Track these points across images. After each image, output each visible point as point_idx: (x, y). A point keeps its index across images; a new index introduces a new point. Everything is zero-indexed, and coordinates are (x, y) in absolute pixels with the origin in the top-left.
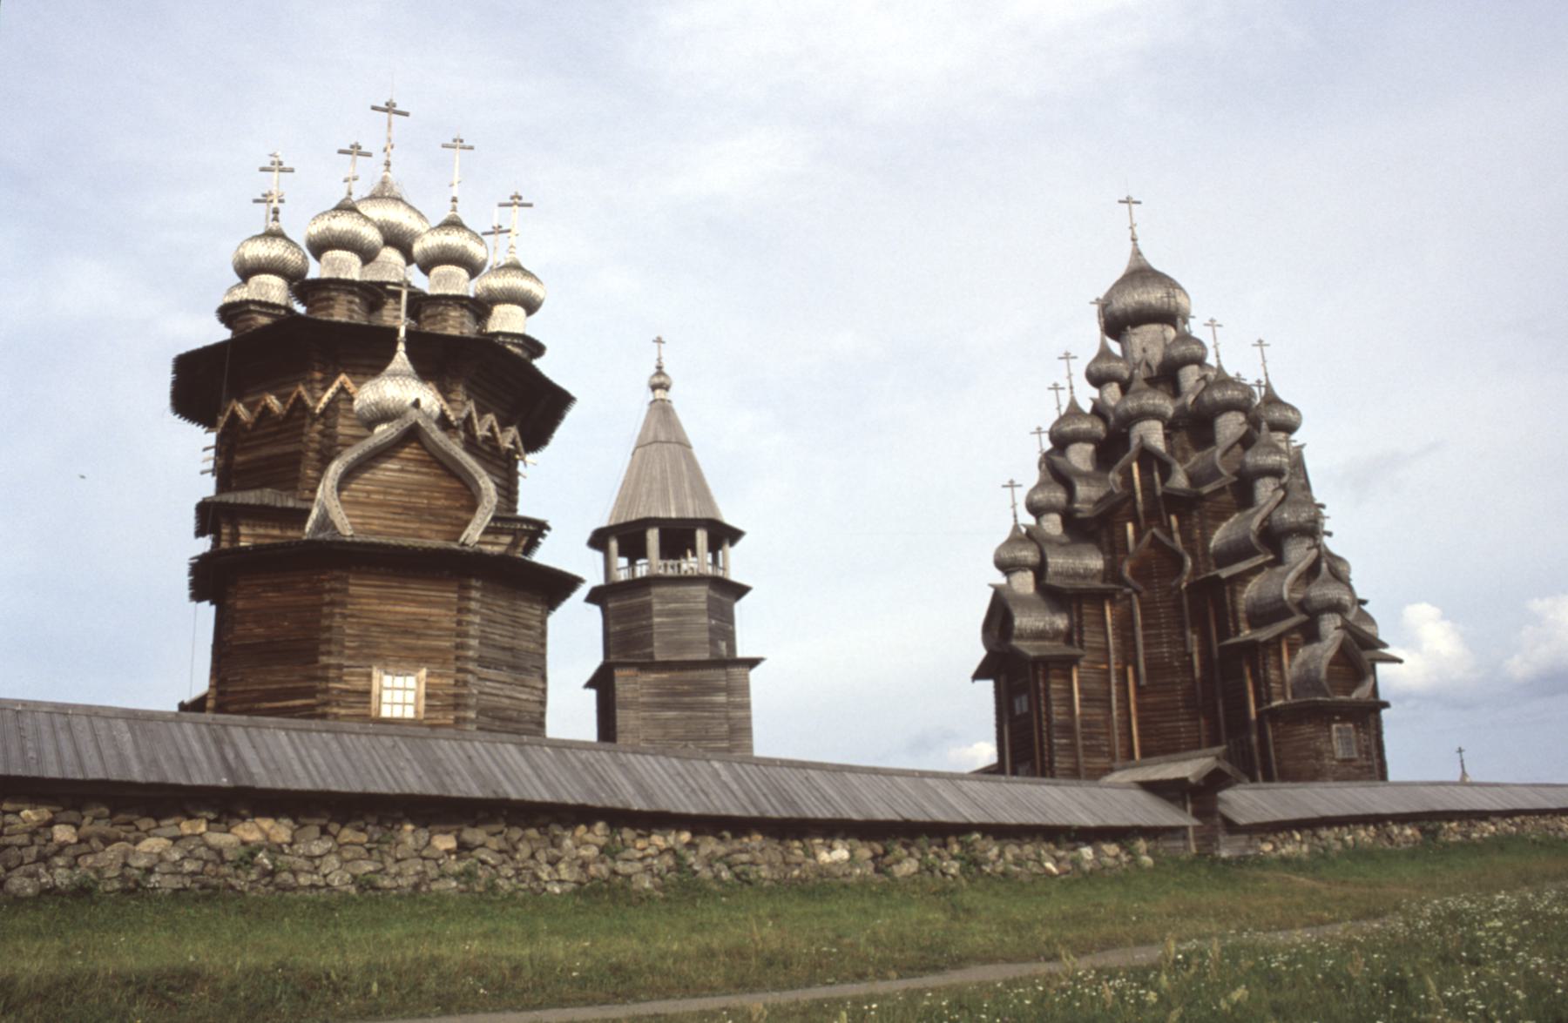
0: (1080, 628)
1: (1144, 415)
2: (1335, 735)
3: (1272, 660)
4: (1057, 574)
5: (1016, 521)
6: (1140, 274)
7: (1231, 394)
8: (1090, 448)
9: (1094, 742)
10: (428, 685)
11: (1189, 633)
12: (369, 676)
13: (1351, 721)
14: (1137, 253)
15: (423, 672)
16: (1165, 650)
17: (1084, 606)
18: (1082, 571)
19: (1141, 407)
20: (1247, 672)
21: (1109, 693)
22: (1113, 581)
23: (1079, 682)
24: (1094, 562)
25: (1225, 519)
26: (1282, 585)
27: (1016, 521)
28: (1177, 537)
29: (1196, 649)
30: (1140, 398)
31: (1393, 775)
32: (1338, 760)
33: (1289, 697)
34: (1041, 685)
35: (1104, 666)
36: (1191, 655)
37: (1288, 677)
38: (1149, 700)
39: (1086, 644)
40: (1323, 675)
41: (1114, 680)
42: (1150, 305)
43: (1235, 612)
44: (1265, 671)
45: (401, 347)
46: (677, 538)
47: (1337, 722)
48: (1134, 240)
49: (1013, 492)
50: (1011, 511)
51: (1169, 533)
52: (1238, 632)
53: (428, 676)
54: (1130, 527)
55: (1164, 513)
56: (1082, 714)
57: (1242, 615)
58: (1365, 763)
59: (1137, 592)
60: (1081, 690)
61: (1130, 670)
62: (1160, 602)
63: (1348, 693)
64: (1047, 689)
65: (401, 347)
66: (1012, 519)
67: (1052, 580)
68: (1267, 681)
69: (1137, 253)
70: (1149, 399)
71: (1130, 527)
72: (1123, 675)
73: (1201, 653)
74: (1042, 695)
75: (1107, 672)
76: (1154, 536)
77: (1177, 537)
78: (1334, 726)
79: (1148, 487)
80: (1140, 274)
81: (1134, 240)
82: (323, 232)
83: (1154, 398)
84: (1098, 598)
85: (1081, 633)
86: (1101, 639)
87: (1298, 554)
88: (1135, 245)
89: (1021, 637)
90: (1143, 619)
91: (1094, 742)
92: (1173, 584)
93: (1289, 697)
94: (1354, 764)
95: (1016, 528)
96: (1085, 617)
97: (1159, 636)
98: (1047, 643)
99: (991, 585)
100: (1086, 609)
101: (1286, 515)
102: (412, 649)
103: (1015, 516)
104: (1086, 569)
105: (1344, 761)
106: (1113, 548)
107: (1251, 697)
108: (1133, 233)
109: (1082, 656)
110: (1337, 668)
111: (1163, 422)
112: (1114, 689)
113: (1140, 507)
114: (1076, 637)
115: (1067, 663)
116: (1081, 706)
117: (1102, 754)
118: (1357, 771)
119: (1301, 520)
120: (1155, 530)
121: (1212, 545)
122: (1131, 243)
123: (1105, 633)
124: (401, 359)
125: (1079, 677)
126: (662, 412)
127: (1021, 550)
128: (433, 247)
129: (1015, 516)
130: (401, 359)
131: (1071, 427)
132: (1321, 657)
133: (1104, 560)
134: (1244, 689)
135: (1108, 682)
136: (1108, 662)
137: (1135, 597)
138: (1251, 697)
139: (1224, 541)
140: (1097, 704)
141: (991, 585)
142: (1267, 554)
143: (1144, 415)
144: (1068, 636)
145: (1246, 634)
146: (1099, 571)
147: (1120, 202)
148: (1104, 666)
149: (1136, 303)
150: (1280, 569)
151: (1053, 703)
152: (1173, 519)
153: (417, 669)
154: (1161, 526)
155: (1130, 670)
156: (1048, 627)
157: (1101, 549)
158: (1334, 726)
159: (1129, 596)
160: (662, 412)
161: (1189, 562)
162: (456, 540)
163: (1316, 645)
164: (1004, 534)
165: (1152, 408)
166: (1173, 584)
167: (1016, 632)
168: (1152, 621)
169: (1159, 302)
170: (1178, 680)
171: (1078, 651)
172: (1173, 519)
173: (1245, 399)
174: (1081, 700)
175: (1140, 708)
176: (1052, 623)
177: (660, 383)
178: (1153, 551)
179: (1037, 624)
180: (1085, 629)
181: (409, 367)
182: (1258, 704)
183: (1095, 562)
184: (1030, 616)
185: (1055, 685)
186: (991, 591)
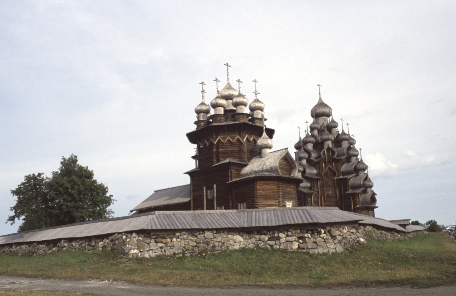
0: (314, 186)
1: (328, 140)
2: (370, 213)
3: (357, 197)
4: (308, 174)
6: (321, 104)
7: (347, 137)
8: (312, 145)
10: (293, 204)
11: (336, 189)
12: (285, 202)
14: (320, 99)
15: (292, 202)
19: (328, 138)
20: (352, 199)
21: (318, 201)
22: (319, 176)
23: (314, 199)
25: (344, 164)
26: (361, 181)
28: (334, 168)
29: (338, 193)
30: (328, 136)
33: (360, 205)
34: (306, 199)
35: (317, 195)
36: (337, 194)
37: (360, 201)
38: (326, 203)
39: (315, 190)
40: (369, 201)
41: (319, 198)
42: (326, 112)
43: (348, 186)
44: (356, 199)
45: (264, 131)
48: (320, 95)
51: (333, 167)
52: (349, 190)
53: (293, 202)
54: (324, 164)
57: (350, 187)
60: (314, 200)
61: (323, 196)
63: (372, 205)
64: (307, 200)
65: (264, 131)
67: (306, 175)
68: (356, 201)
69: (320, 99)
71: (324, 164)
72: (321, 197)
73: (339, 194)
74: (306, 201)
75: (318, 197)
76: (329, 167)
77: (334, 168)
79: (329, 156)
80: (321, 104)
81: (320, 95)
82: (241, 102)
84: (317, 180)
85: (314, 188)
86: (317, 189)
87: (361, 174)
89: (301, 188)
92: (334, 178)
93: (360, 205)
97: (329, 189)
101: (361, 166)
102: (289, 197)
106: (319, 169)
107: (352, 204)
109: (314, 193)
112: (319, 201)
113: (326, 160)
114: (313, 189)
115: (311, 195)
116: (314, 204)
119: (364, 167)
120: (330, 166)
121: (341, 170)
122: (319, 96)
123: (318, 189)
124: (264, 133)
127: (300, 168)
128: (257, 107)
130: (264, 133)
131: (310, 140)
132: (369, 197)
133: (317, 171)
134: (351, 202)
135: (318, 199)
136: (318, 195)
138: (352, 204)
139: (345, 170)
142: (355, 174)
143: (328, 140)
144: (310, 188)
145: (350, 191)
148: (317, 195)
150: (358, 177)
151: (309, 203)
152: (334, 163)
153: (291, 201)
154: (331, 165)
155: (323, 196)
157: (316, 169)
158: (370, 211)
161: (337, 173)
162: (290, 174)
163: (366, 194)
166: (334, 178)
167: (300, 186)
168: (328, 186)
170: (333, 199)
171: (313, 192)
172: (334, 163)
176: (307, 185)
178: (328, 170)
180: (315, 187)
181: (267, 136)
182: (354, 207)
183: (315, 171)
185: (309, 199)
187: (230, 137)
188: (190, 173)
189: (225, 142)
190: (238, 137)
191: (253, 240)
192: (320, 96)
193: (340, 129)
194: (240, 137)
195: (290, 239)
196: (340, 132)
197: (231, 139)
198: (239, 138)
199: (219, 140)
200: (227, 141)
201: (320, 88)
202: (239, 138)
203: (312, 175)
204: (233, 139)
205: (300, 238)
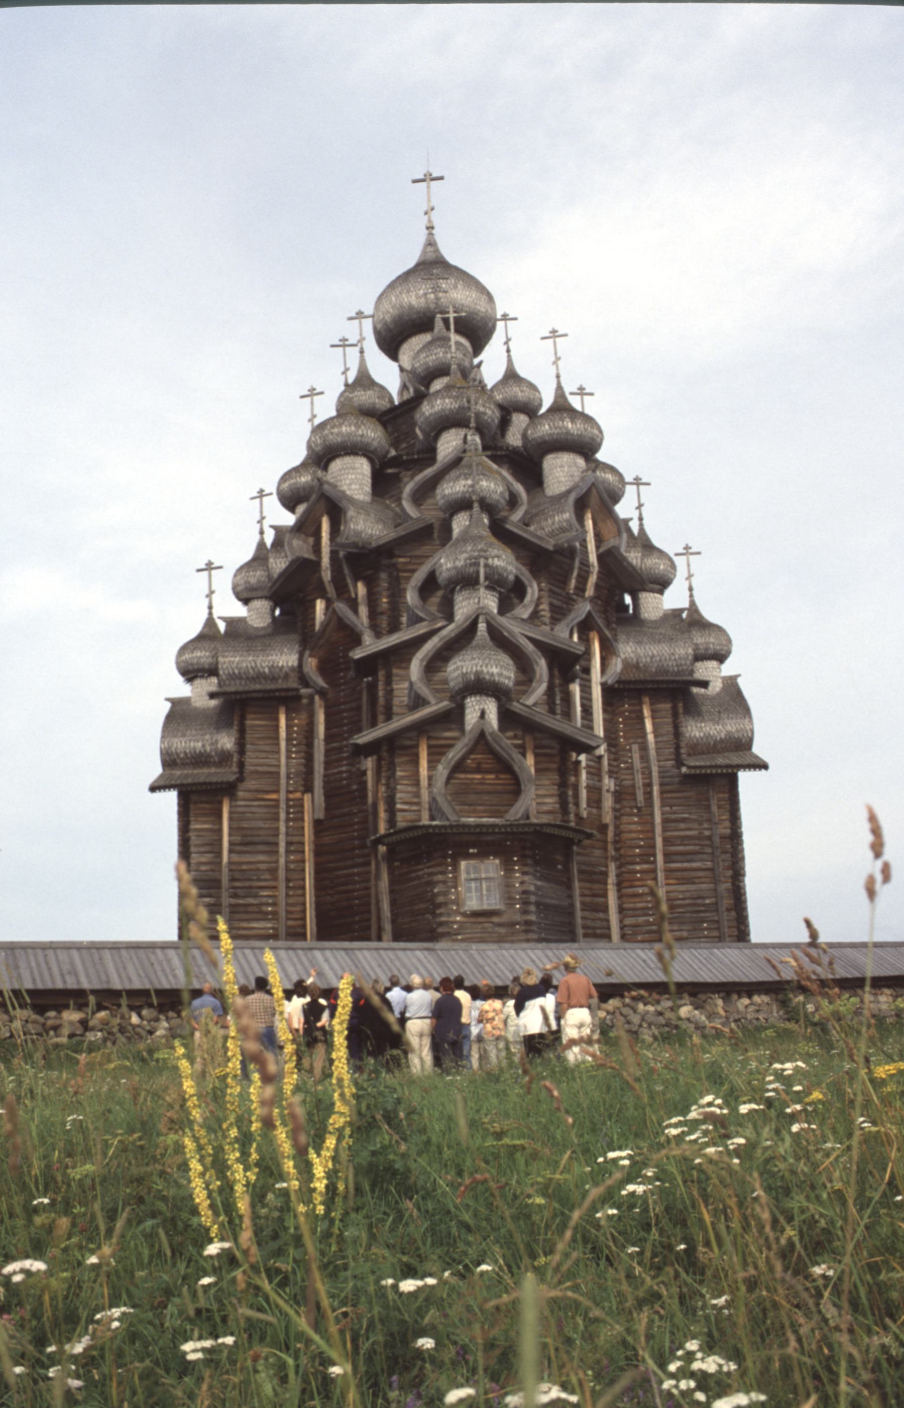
5: (210, 614)
9: (251, 901)
13: (495, 857)
14: (431, 243)
16: (344, 769)
17: (249, 716)
18: (267, 670)
23: (231, 819)
24: (284, 657)
27: (210, 614)
28: (363, 610)
31: (756, 936)
32: (464, 914)
42: (411, 307)
47: (468, 856)
49: (210, 576)
50: (206, 602)
55: (349, 581)
56: (230, 863)
58: (518, 918)
59: (322, 693)
62: (344, 703)
66: (206, 611)
69: (431, 243)
70: (333, 427)
78: (463, 864)
83: (340, 425)
88: (431, 234)
90: (327, 728)
91: (251, 901)
94: (496, 919)
95: (210, 622)
96: (248, 731)
98: (213, 770)
99: (167, 699)
100: (252, 722)
103: (210, 607)
104: (271, 668)
105: (476, 914)
108: (430, 221)
110: (479, 776)
111: (371, 461)
117: (264, 916)
118: (502, 930)
119: (459, 564)
125: (231, 813)
129: (210, 607)
137: (317, 698)
140: (261, 848)
141: (167, 699)
146: (292, 669)
147: (415, 181)
149: (394, 307)
156: (208, 748)
158: (463, 864)
159: (311, 698)
164: (195, 628)
165: (339, 439)
169: (423, 300)
173: (461, 408)
174: (231, 844)
175: (318, 852)
179: (192, 744)
180: (248, 746)
184: (184, 735)
186: (168, 705)
201: (432, 190)
203: (273, 678)
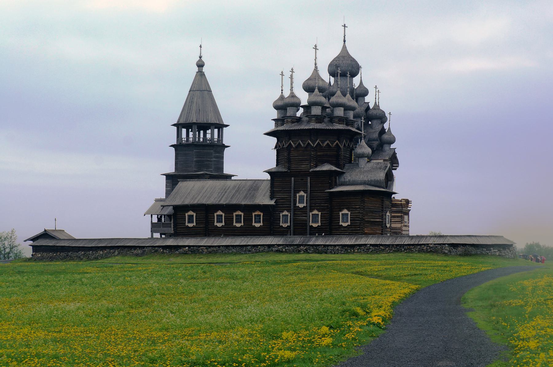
6: (344, 55)
14: (344, 47)
46: (204, 127)
69: (344, 47)
80: (344, 55)
81: (345, 41)
126: (201, 74)
160: (201, 74)
177: (200, 65)
187: (329, 141)
188: (270, 172)
189: (324, 146)
190: (337, 141)
191: (479, 250)
192: (345, 43)
193: (370, 99)
194: (339, 142)
195: (495, 250)
196: (371, 106)
197: (330, 143)
198: (338, 143)
199: (319, 143)
200: (326, 145)
202: (338, 143)
204: (332, 144)
205: (499, 250)
